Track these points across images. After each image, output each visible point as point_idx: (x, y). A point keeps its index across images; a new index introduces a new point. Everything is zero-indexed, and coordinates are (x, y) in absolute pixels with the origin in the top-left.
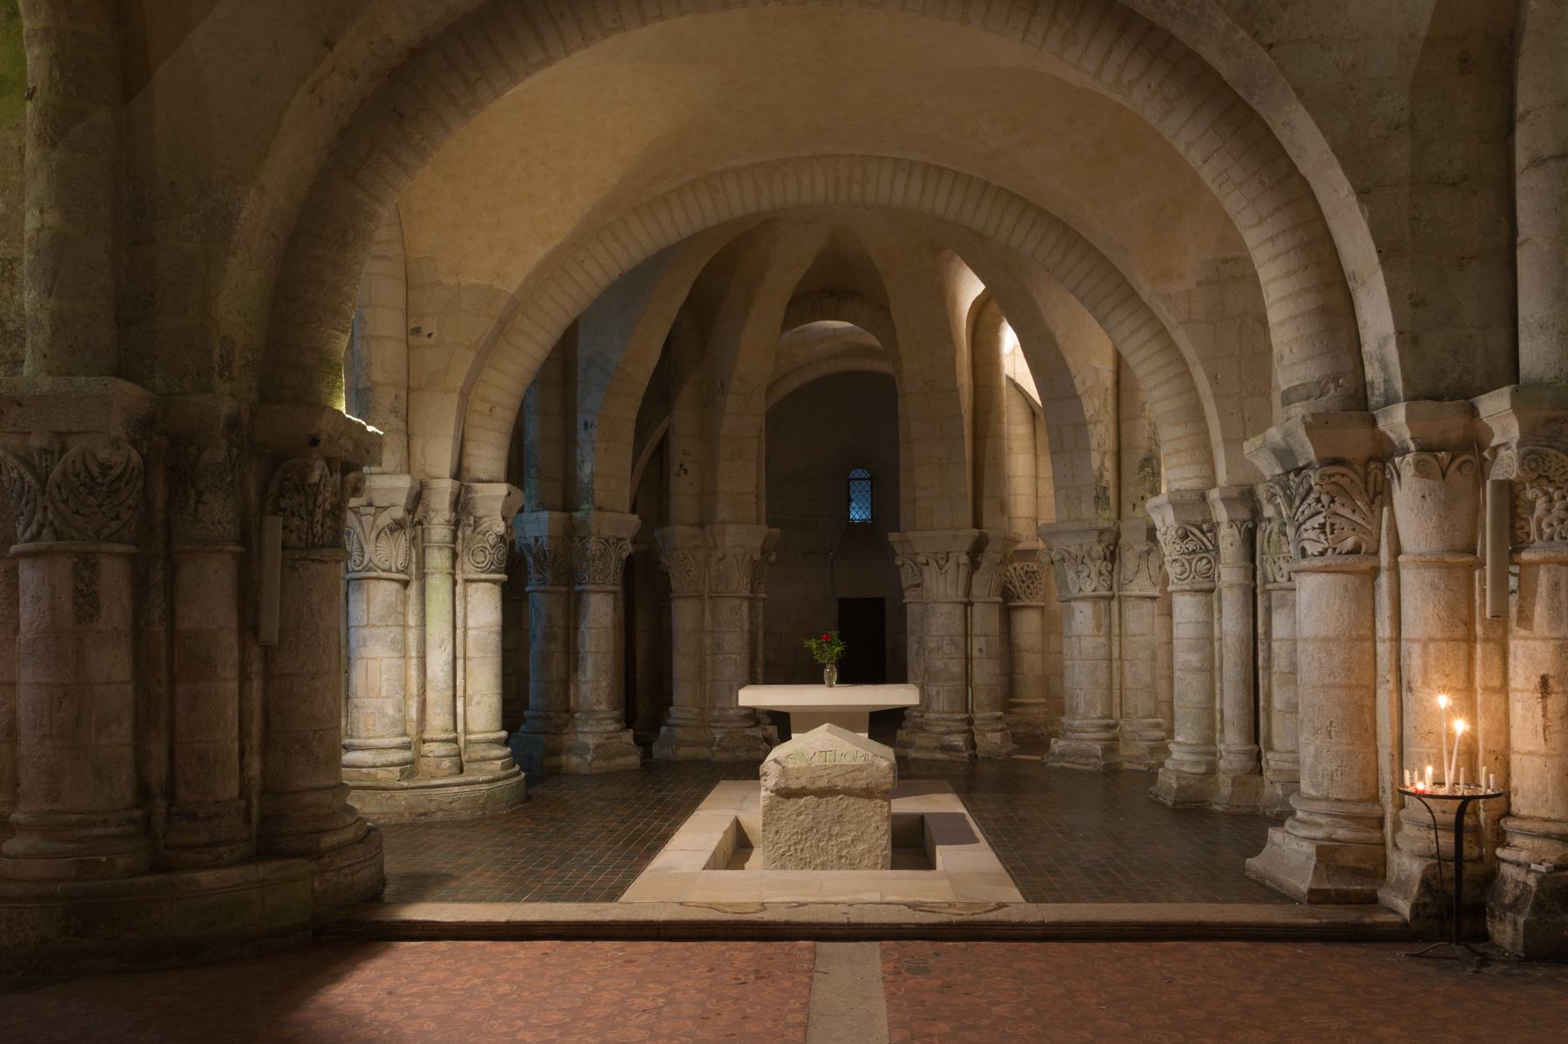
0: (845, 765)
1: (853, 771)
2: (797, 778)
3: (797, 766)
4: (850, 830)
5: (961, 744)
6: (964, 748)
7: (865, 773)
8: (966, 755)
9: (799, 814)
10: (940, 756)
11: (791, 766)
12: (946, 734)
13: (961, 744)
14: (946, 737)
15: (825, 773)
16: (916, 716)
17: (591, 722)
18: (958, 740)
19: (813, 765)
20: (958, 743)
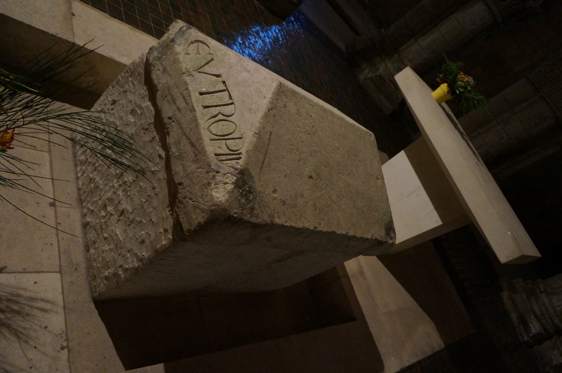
0: (197, 126)
1: (192, 145)
2: (165, 70)
3: (181, 57)
4: (131, 199)
5: (534, 331)
6: (531, 335)
7: (194, 166)
8: (526, 338)
9: (133, 112)
10: (514, 316)
11: (178, 48)
12: (536, 316)
13: (534, 331)
14: (532, 317)
15: (181, 103)
16: (540, 288)
17: (396, 65)
18: (535, 328)
19: (188, 79)
20: (533, 329)
